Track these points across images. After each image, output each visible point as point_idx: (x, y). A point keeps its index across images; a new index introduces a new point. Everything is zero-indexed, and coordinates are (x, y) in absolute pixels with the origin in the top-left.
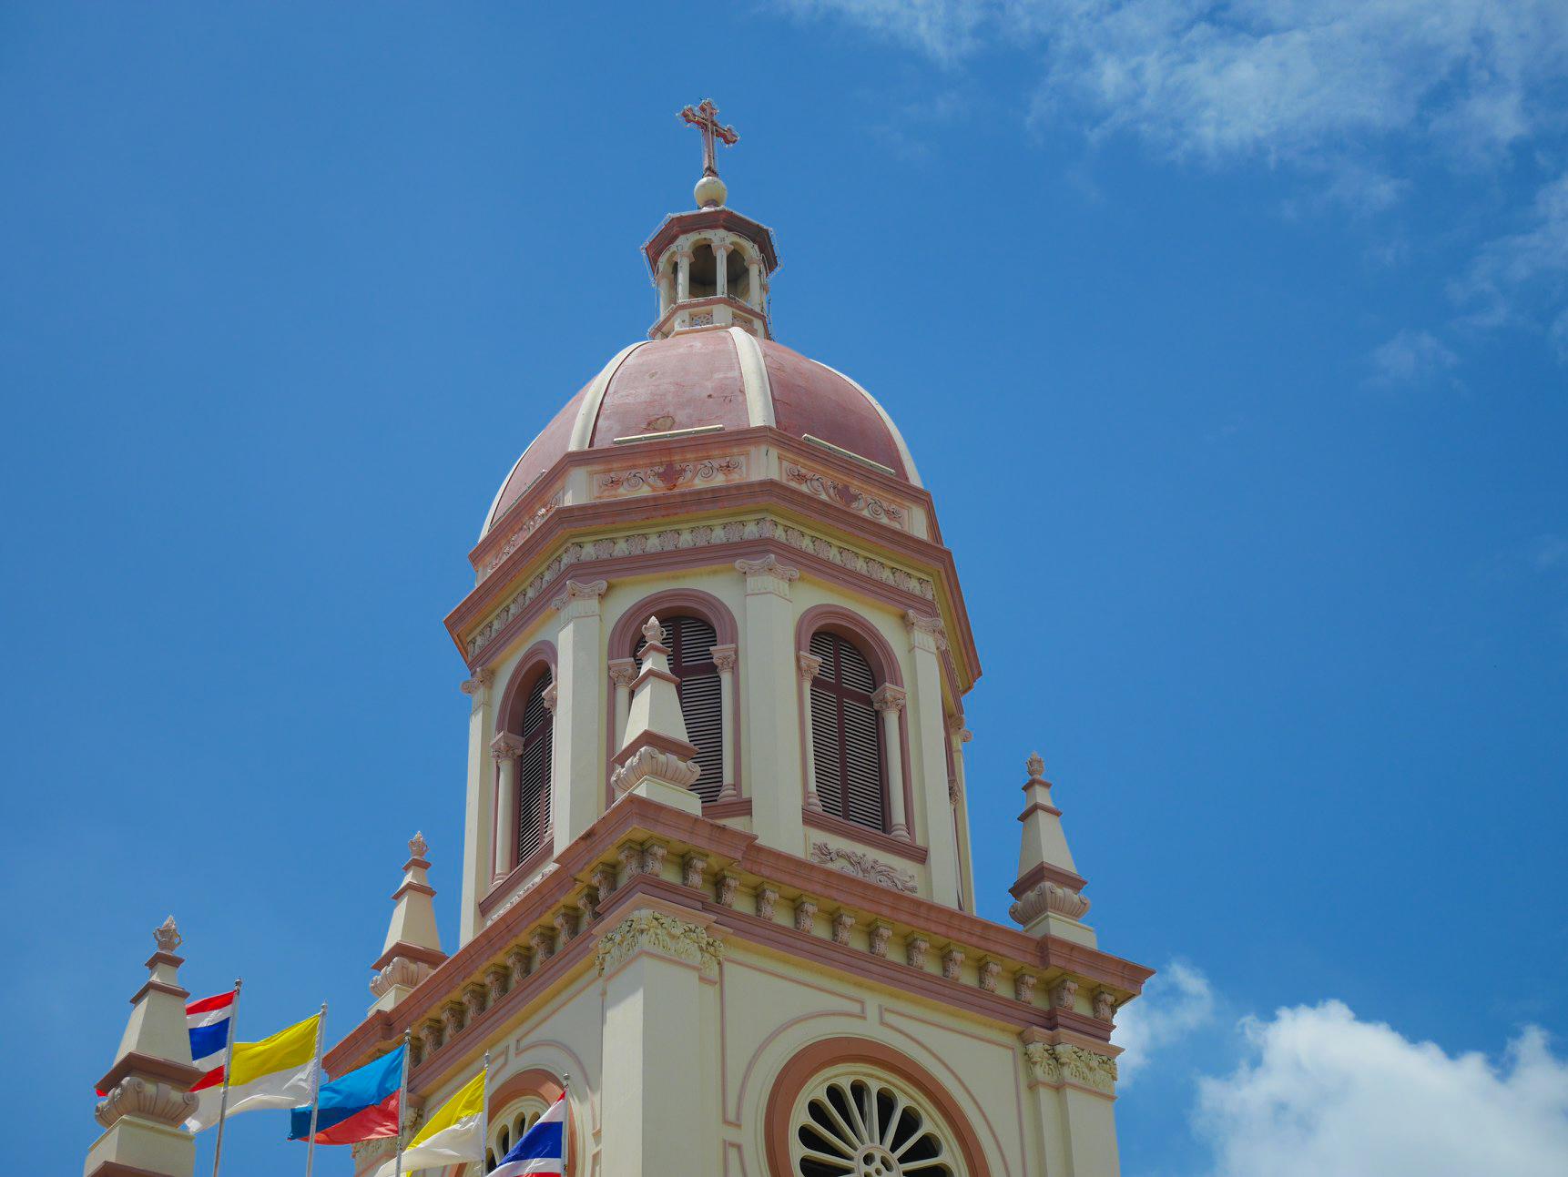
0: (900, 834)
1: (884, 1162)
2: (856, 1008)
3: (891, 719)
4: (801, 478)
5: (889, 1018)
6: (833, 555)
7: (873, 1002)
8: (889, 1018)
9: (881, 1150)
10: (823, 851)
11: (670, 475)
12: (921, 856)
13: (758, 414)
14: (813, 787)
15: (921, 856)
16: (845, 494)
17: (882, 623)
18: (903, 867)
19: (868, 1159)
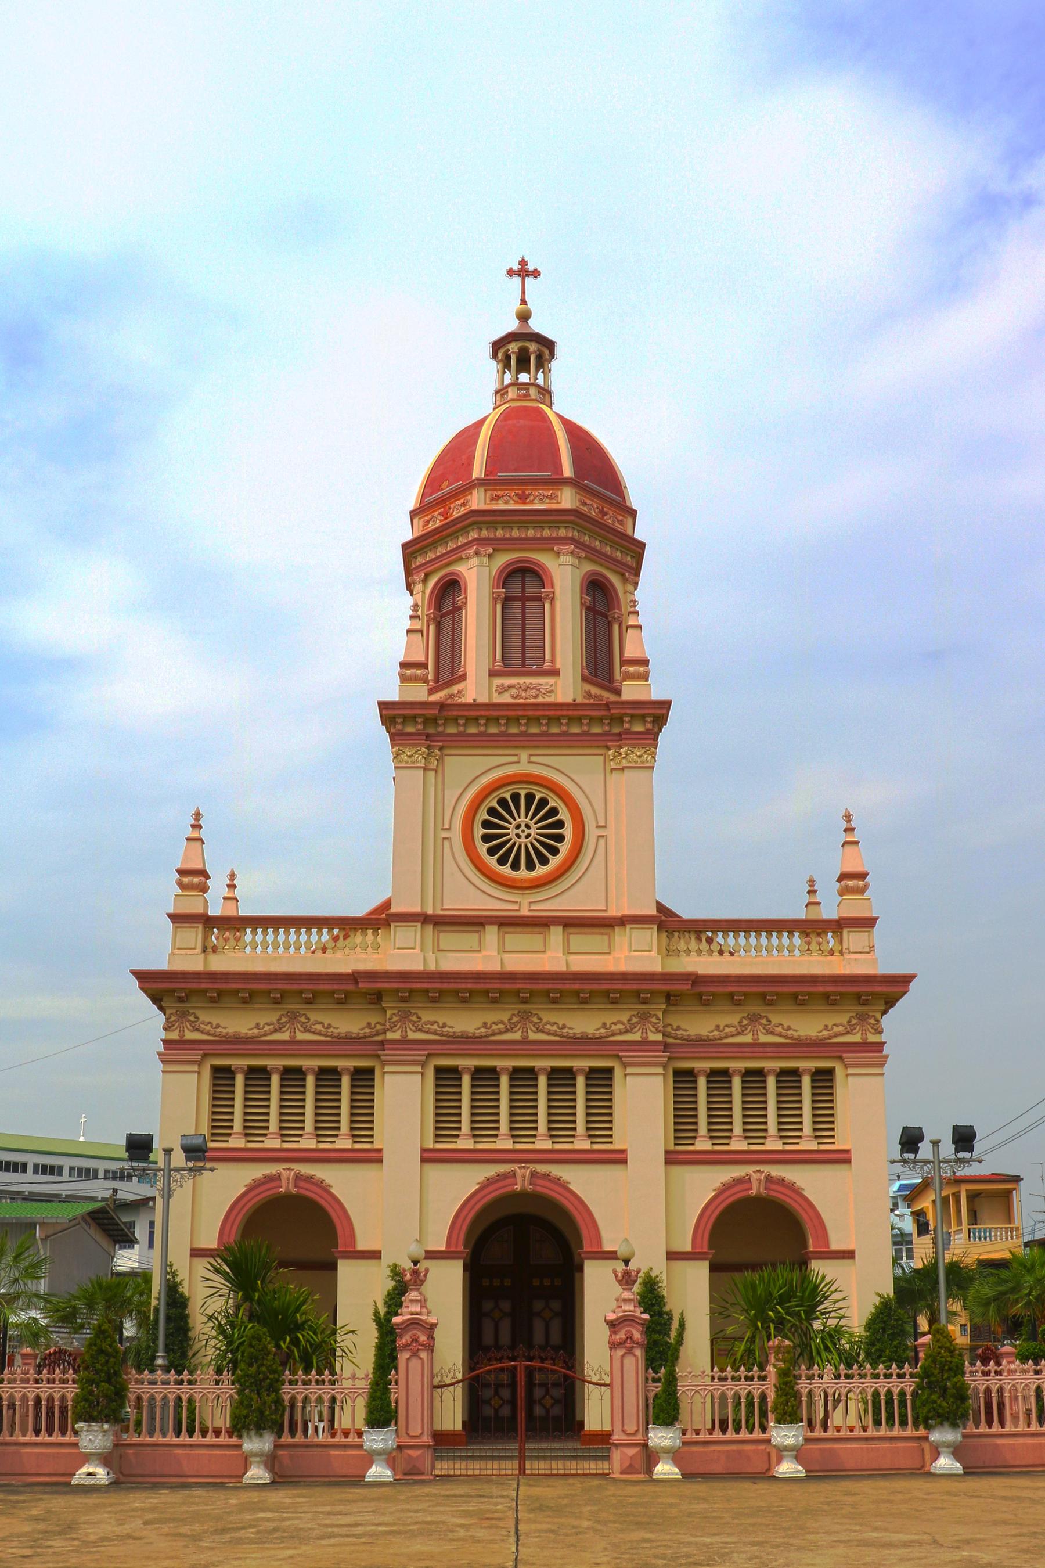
0: (547, 665)
1: (528, 827)
2: (515, 759)
3: (547, 606)
4: (498, 498)
5: (533, 759)
6: (515, 533)
7: (524, 755)
8: (533, 759)
9: (522, 819)
10: (502, 690)
11: (445, 515)
12: (555, 673)
13: (478, 471)
14: (499, 656)
15: (555, 673)
16: (523, 498)
17: (544, 559)
18: (549, 681)
19: (518, 827)
